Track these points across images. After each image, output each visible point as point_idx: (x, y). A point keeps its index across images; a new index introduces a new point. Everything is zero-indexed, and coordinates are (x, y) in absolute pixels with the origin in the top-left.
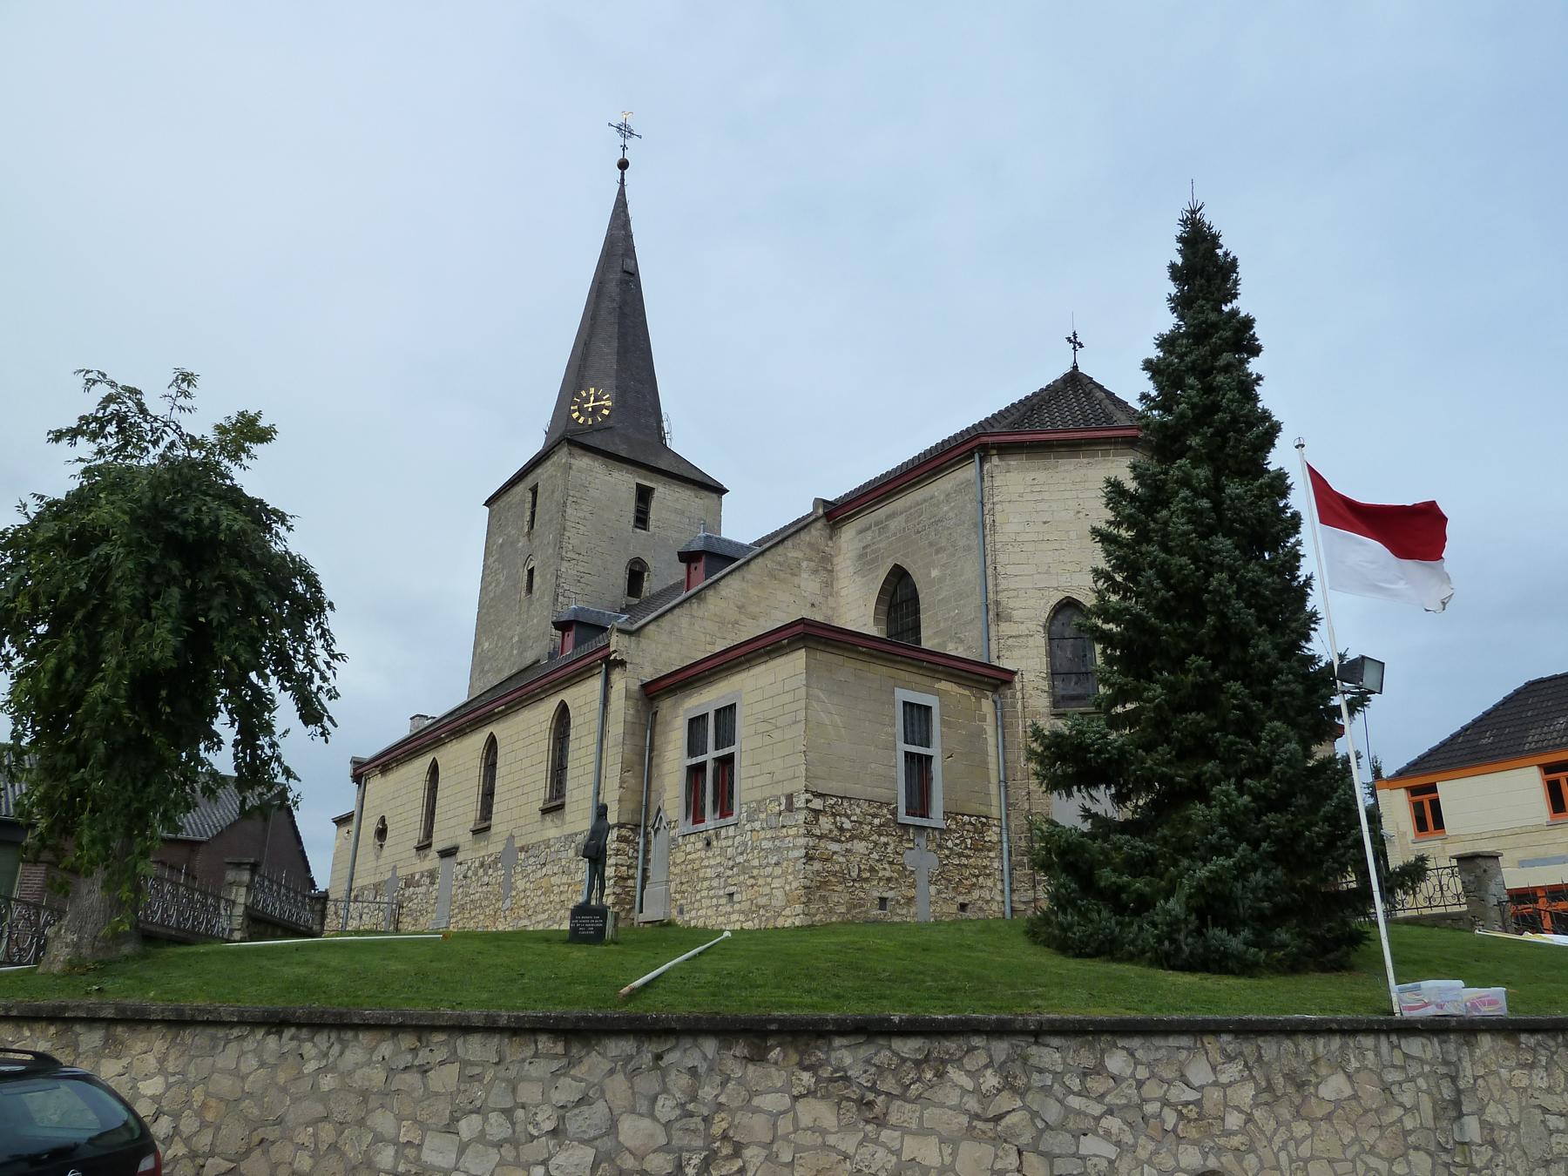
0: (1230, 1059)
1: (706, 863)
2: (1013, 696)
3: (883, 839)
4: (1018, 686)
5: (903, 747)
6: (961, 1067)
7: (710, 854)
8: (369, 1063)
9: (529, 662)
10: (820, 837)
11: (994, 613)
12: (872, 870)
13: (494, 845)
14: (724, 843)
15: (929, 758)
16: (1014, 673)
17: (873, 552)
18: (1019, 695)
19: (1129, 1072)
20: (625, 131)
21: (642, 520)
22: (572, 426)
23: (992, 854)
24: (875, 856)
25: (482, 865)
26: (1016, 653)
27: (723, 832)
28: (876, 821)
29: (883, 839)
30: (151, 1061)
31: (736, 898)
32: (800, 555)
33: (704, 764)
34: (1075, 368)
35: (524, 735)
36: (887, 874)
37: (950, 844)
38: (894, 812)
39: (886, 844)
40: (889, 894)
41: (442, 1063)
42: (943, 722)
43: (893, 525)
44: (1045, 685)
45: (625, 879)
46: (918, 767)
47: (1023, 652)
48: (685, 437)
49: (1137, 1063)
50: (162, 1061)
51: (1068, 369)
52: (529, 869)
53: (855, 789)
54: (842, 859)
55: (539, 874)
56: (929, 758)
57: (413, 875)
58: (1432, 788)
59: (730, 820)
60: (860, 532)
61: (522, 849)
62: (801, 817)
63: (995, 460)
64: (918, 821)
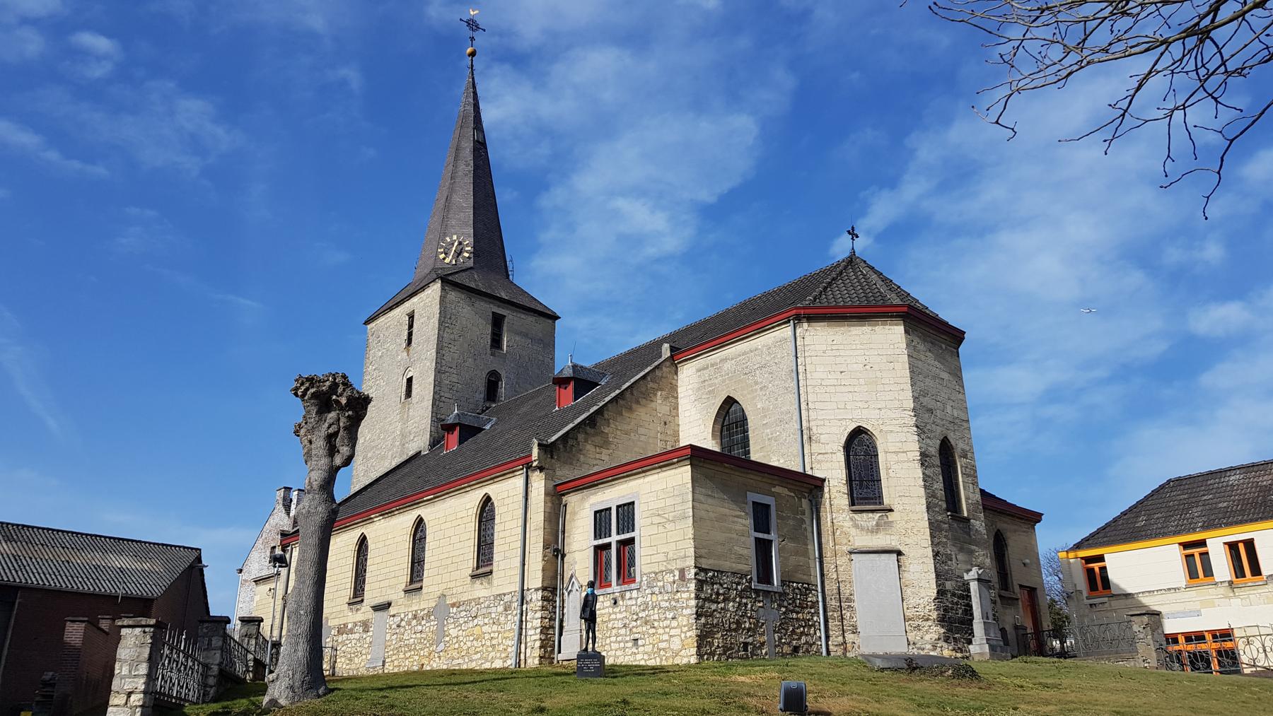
1: (613, 616)
4: (826, 490)
7: (617, 610)
9: (411, 453)
10: (705, 600)
11: (805, 436)
13: (424, 602)
14: (630, 603)
15: (770, 542)
17: (710, 386)
22: (439, 265)
25: (415, 617)
26: (825, 466)
31: (640, 642)
33: (608, 546)
35: (450, 518)
40: (750, 640)
42: (779, 517)
43: (727, 366)
44: (845, 489)
45: (548, 629)
46: (763, 549)
47: (829, 465)
51: (847, 254)
52: (461, 620)
53: (726, 565)
55: (471, 625)
56: (770, 542)
57: (345, 625)
58: (1100, 558)
59: (633, 586)
60: (699, 370)
61: (453, 605)
62: (692, 586)
63: (805, 325)
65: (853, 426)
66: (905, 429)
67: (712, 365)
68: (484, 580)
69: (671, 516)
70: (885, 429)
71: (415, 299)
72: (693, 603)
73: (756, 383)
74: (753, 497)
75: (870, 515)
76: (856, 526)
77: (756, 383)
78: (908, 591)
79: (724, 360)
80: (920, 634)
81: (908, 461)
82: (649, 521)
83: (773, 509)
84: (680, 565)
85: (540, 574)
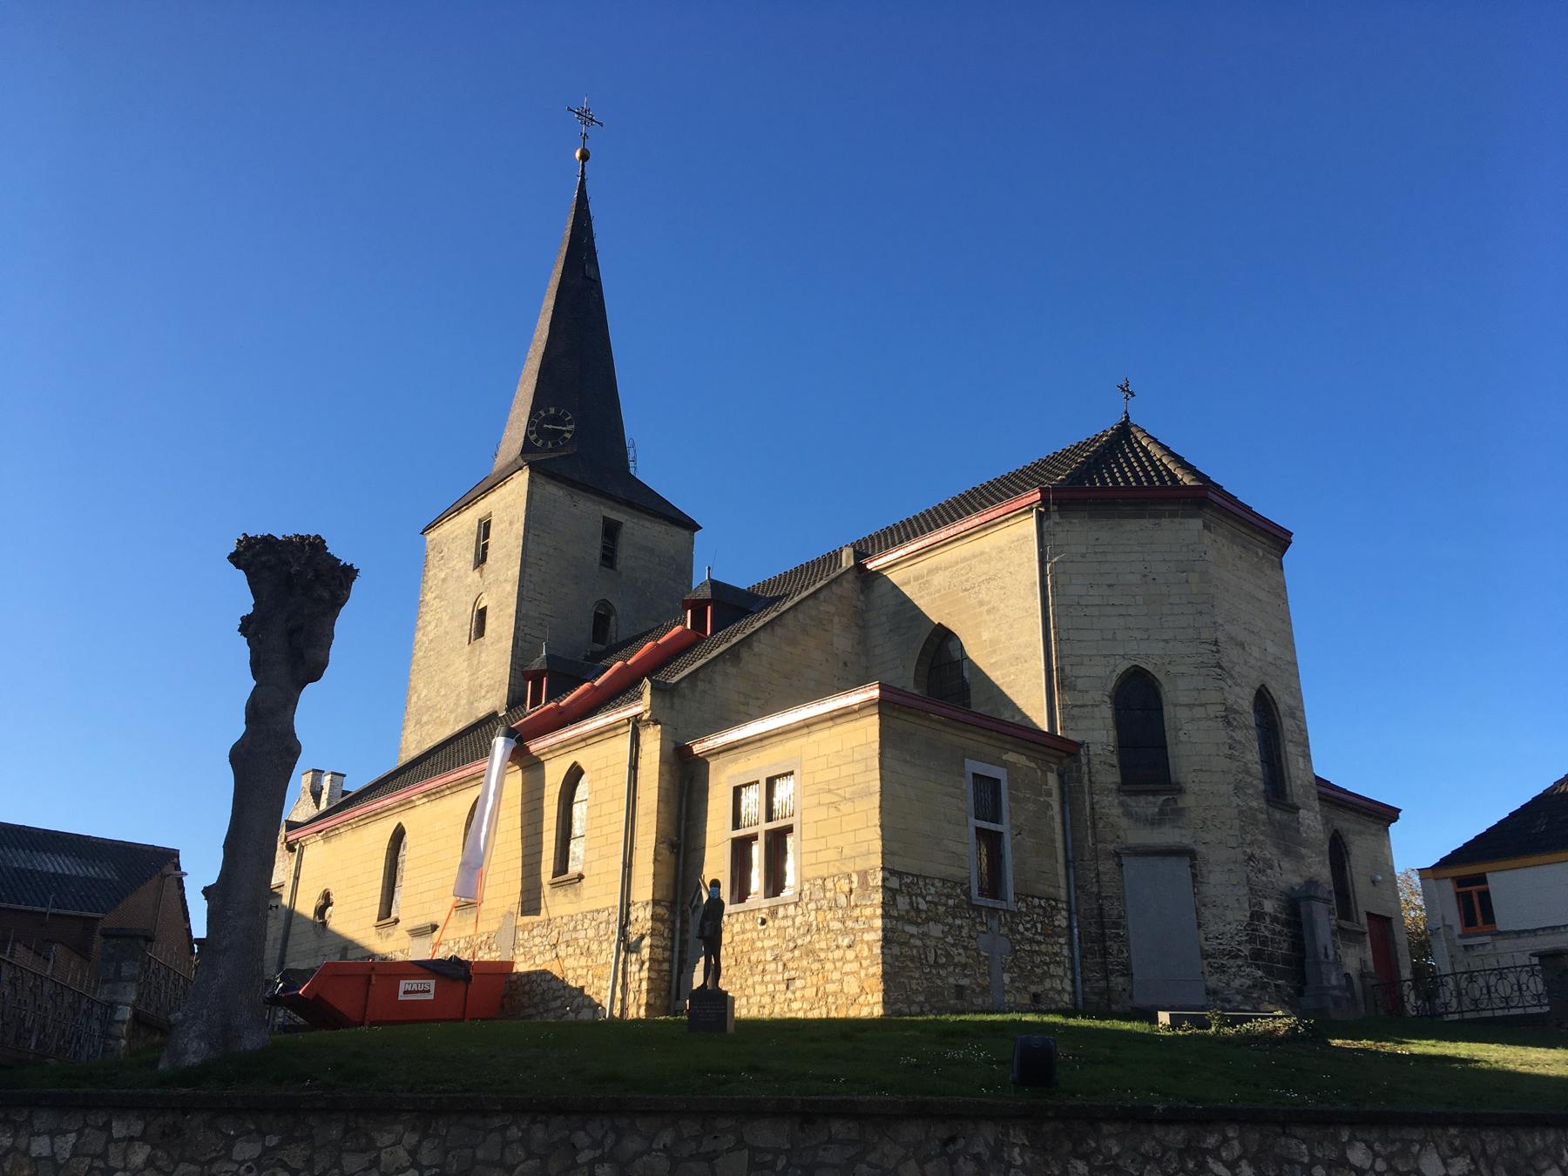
0: (1457, 1152)
2: (1079, 769)
3: (958, 922)
4: (1084, 760)
5: (972, 820)
6: (1218, 1158)
8: (649, 1151)
9: (481, 714)
12: (948, 955)
16: (1079, 745)
18: (1085, 769)
19: (1367, 1165)
20: (586, 117)
21: (608, 558)
23: (1062, 940)
24: (950, 939)
27: (781, 912)
28: (951, 902)
29: (958, 922)
30: (403, 1157)
32: (832, 609)
34: (1127, 417)
36: (963, 960)
37: (1021, 928)
38: (967, 893)
39: (961, 927)
40: (965, 982)
41: (729, 1150)
42: (1013, 798)
44: (1114, 760)
48: (650, 466)
49: (1376, 1155)
50: (413, 1152)
54: (919, 943)
58: (1481, 879)
62: (878, 897)
64: (990, 902)
65: (1124, 666)
66: (1204, 671)
67: (916, 579)
68: (570, 892)
69: (848, 793)
70: (1173, 669)
71: (492, 498)
72: (878, 923)
73: (981, 603)
74: (974, 766)
75: (1151, 798)
76: (1128, 814)
77: (981, 603)
78: (1207, 914)
79: (931, 572)
80: (1224, 978)
81: (1208, 718)
82: (814, 800)
83: (1004, 785)
84: (861, 865)
85: (650, 881)
